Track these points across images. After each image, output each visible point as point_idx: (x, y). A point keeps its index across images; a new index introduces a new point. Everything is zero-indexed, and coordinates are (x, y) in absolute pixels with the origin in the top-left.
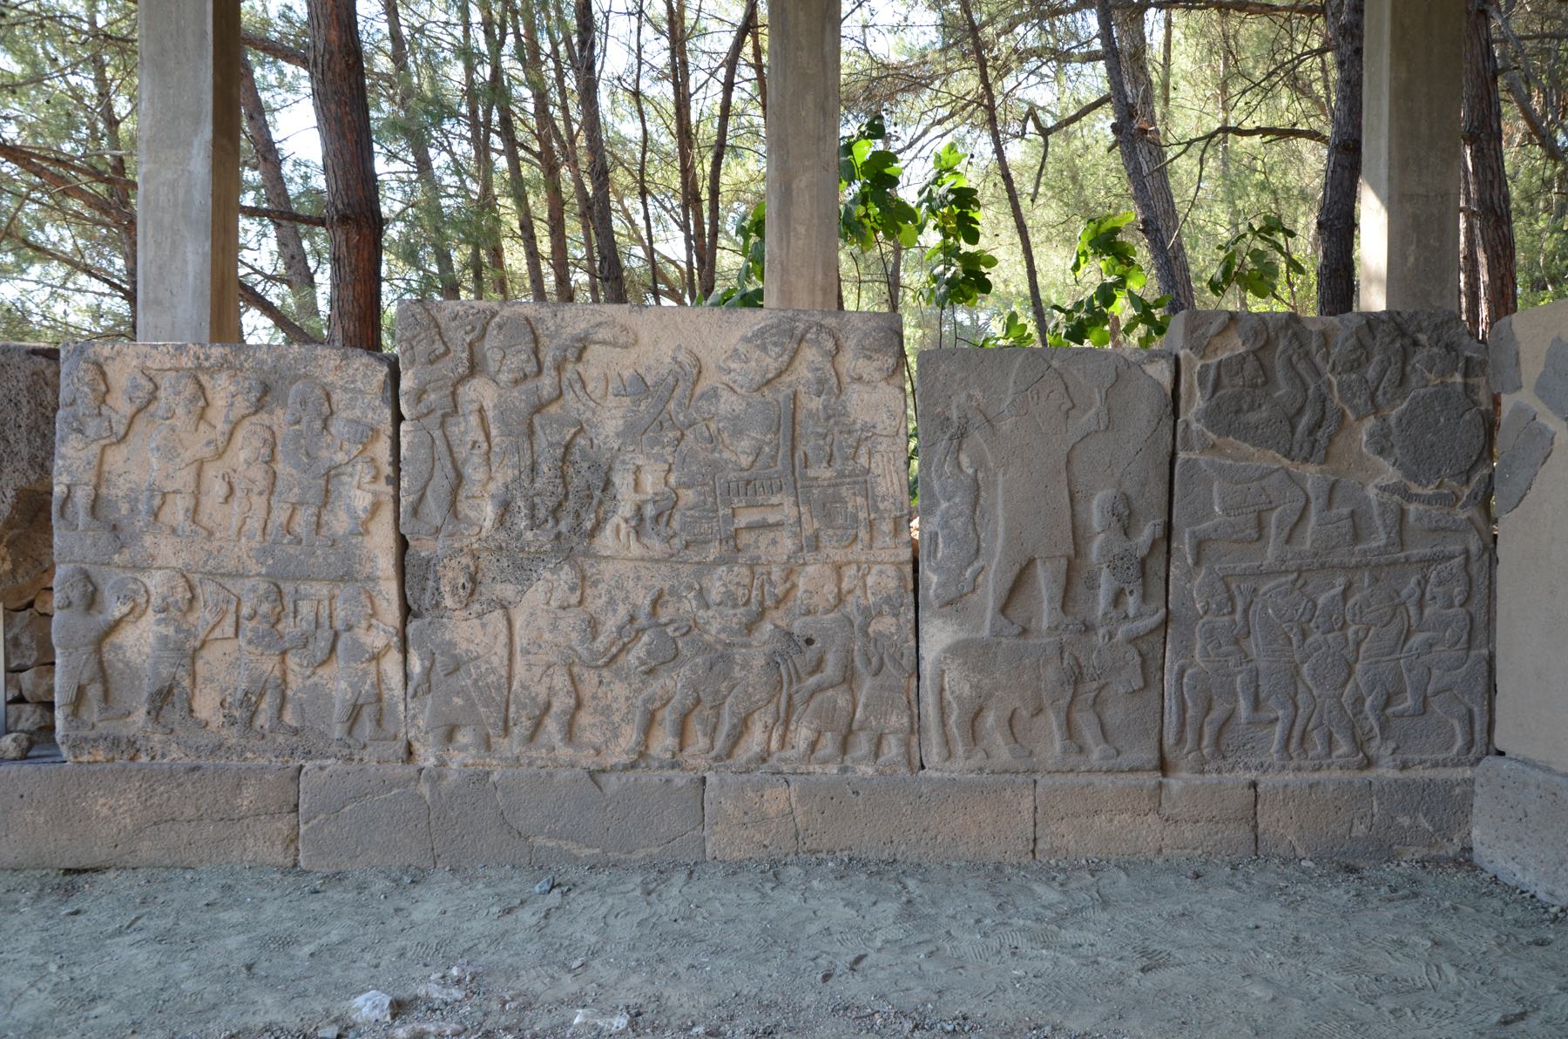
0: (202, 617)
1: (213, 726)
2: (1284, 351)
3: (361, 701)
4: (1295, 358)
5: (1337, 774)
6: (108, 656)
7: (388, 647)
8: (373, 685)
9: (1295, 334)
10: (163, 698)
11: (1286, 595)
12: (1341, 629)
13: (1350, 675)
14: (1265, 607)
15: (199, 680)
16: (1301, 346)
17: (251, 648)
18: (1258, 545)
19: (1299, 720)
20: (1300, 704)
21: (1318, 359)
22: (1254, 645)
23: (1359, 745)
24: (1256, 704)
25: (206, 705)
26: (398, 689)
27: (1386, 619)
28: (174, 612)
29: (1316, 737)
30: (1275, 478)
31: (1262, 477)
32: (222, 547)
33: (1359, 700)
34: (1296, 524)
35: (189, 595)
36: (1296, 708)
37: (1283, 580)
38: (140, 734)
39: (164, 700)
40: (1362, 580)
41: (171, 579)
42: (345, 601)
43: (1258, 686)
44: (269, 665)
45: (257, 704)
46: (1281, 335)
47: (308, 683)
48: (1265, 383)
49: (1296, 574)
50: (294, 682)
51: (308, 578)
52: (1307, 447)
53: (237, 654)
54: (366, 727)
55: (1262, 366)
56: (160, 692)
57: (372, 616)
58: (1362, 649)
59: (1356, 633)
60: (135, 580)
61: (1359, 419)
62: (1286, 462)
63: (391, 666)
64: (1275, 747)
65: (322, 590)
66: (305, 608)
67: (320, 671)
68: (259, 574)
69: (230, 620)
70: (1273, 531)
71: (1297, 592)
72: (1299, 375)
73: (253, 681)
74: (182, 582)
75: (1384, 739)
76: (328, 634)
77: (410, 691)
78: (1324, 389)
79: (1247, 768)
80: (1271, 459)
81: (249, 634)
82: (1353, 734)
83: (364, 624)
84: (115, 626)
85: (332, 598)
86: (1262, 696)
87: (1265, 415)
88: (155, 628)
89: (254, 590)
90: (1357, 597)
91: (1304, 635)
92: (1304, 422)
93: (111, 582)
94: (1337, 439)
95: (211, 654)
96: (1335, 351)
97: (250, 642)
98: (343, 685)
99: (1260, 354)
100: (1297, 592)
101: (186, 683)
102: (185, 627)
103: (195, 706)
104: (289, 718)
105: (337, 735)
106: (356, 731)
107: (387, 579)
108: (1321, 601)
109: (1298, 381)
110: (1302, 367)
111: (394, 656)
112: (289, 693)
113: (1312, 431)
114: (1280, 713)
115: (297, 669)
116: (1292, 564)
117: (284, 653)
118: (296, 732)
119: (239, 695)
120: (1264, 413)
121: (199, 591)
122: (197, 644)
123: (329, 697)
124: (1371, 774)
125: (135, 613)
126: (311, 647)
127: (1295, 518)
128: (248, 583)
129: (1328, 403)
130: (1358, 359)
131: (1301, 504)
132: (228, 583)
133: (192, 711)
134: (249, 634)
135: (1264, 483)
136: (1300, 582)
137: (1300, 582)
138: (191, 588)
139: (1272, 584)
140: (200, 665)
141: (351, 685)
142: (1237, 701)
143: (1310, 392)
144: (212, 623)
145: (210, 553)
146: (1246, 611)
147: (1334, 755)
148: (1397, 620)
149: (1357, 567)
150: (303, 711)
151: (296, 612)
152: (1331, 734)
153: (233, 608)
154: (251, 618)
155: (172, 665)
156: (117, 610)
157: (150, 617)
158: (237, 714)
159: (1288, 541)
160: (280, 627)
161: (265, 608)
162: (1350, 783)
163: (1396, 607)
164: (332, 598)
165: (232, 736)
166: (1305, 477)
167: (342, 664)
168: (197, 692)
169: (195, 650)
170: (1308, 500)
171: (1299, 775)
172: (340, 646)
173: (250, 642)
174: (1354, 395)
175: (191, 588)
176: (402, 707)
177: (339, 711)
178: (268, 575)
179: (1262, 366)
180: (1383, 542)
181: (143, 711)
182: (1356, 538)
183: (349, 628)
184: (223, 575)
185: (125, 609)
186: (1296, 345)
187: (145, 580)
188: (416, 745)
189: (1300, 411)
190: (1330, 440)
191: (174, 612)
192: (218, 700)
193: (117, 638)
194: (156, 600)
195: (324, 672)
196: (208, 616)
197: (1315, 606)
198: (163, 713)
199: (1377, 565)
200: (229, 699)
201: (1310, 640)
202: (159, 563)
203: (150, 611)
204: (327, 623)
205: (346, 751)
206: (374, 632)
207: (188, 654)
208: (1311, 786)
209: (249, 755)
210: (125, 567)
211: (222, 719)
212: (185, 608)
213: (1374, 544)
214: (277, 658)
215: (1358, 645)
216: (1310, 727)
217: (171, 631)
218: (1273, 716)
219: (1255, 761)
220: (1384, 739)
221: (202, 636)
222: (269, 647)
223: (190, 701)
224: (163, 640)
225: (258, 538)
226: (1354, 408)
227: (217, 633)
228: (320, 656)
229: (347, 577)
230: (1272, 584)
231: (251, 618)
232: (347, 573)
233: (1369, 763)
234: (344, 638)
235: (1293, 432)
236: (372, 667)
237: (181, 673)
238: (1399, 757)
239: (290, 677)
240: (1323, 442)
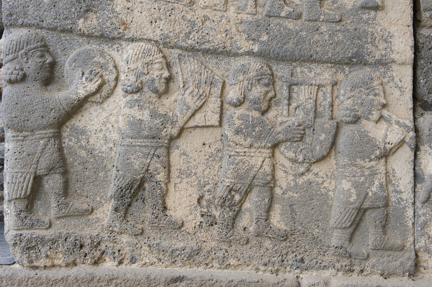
0: (176, 103)
1: (189, 226)
3: (367, 204)
6: (69, 142)
7: (402, 142)
8: (381, 186)
10: (132, 194)
15: (174, 173)
17: (239, 139)
25: (181, 203)
26: (407, 195)
28: (148, 94)
32: (206, 18)
35: (166, 74)
38: (105, 235)
39: (134, 196)
41: (147, 53)
42: (353, 88)
44: (258, 159)
45: (241, 202)
47: (301, 181)
50: (284, 180)
51: (310, 60)
53: (218, 145)
54: (370, 235)
56: (130, 186)
57: (384, 106)
60: (102, 54)
63: (401, 164)
65: (326, 75)
66: (303, 95)
67: (315, 169)
68: (250, 53)
69: (213, 104)
73: (239, 177)
74: (158, 58)
76: (329, 125)
77: (422, 193)
81: (238, 123)
83: (375, 115)
84: (78, 107)
85: (335, 84)
88: (127, 111)
89: (244, 70)
93: (72, 55)
95: (190, 144)
97: (238, 132)
98: (346, 185)
101: (161, 177)
102: (161, 111)
103: (169, 203)
104: (277, 220)
105: (334, 241)
106: (357, 238)
107: (403, 64)
111: (406, 153)
112: (278, 191)
115: (288, 164)
117: (275, 146)
118: (285, 237)
119: (221, 191)
121: (176, 69)
122: (175, 132)
123: (325, 199)
125: (99, 95)
126: (308, 140)
128: (236, 63)
132: (211, 62)
133: (165, 208)
134: (238, 123)
138: (169, 66)
140: (175, 155)
141: (356, 185)
144: (193, 107)
145: (193, 24)
150: (293, 211)
151: (290, 98)
153: (217, 91)
154: (239, 104)
155: (146, 155)
156: (78, 86)
157: (119, 99)
158: (217, 213)
160: (271, 114)
161: (257, 92)
164: (335, 84)
165: (210, 239)
167: (344, 160)
168: (171, 187)
169: (172, 139)
172: (342, 140)
173: (238, 132)
175: (169, 66)
176: (410, 213)
177: (337, 215)
178: (260, 55)
181: (109, 207)
183: (356, 120)
184: (206, 52)
185: (92, 87)
187: (114, 53)
188: (423, 256)
191: (148, 94)
192: (196, 197)
193: (80, 121)
194: (127, 79)
195: (321, 169)
196: (188, 99)
198: (132, 209)
200: (207, 197)
202: (129, 35)
203: (119, 90)
204: (327, 113)
205: (346, 262)
206: (383, 125)
207: (163, 140)
209: (233, 262)
210: (90, 36)
211: (199, 219)
212: (162, 89)
214: (267, 152)
217: (145, 115)
221: (180, 123)
222: (258, 138)
223: (164, 196)
224: (136, 125)
225: (249, 9)
227: (199, 119)
228: (319, 150)
229: (356, 60)
231: (239, 104)
232: (356, 55)
234: (347, 131)
236: (381, 166)
237: (156, 165)
239: (280, 174)
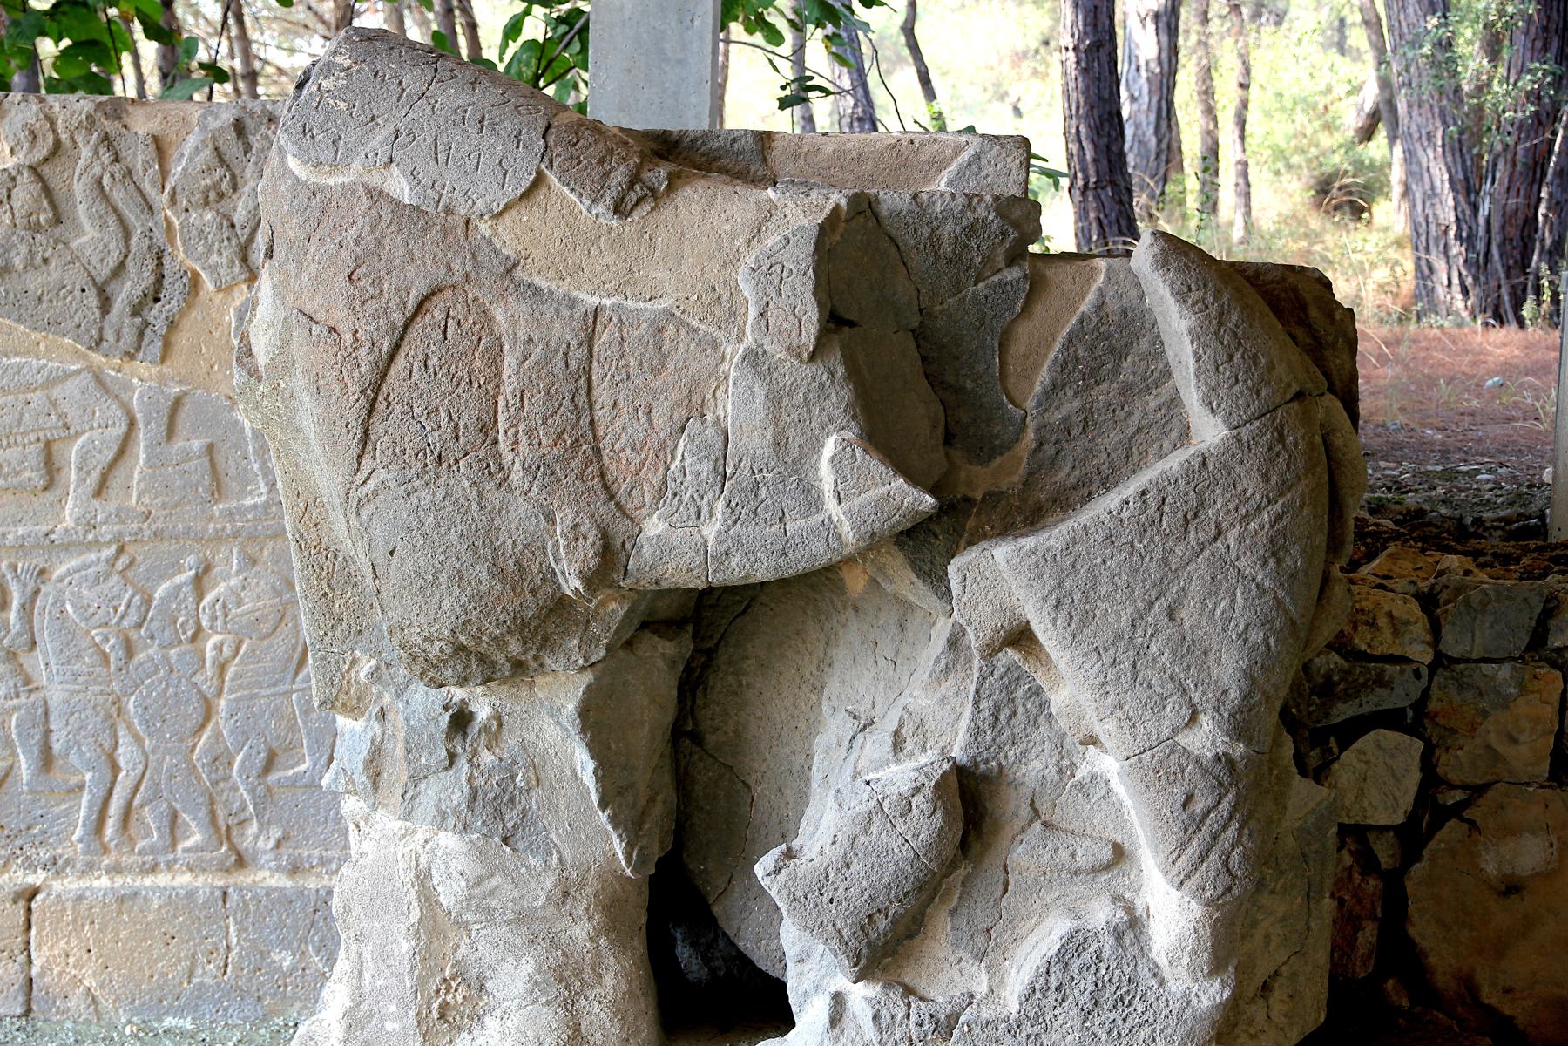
2: (87, 168)
4: (106, 181)
5: (184, 879)
9: (106, 139)
11: (97, 581)
12: (194, 639)
13: (207, 717)
14: (58, 602)
16: (117, 160)
18: (50, 497)
19: (118, 789)
20: (122, 762)
21: (147, 186)
22: (44, 665)
23: (223, 832)
24: (46, 759)
27: (265, 628)
29: (150, 818)
30: (72, 388)
31: (50, 383)
33: (220, 760)
34: (112, 465)
36: (115, 768)
37: (93, 556)
40: (228, 561)
43: (48, 732)
46: (79, 139)
48: (58, 220)
49: (113, 548)
52: (129, 334)
55: (47, 191)
58: (231, 670)
59: (219, 648)
61: (225, 289)
62: (97, 358)
64: (79, 832)
70: (73, 477)
71: (116, 578)
72: (115, 210)
75: (264, 827)
78: (160, 238)
79: (31, 866)
80: (62, 355)
82: (213, 813)
86: (57, 747)
87: (55, 275)
90: (221, 588)
91: (129, 649)
92: (126, 292)
94: (186, 324)
96: (177, 170)
99: (46, 171)
100: (116, 578)
108: (160, 592)
109: (111, 219)
110: (118, 195)
113: (136, 311)
114: (88, 776)
116: (106, 532)
120: (54, 272)
124: (245, 878)
127: (110, 455)
129: (166, 260)
130: (216, 185)
131: (122, 429)
135: (56, 392)
136: (123, 561)
137: (123, 561)
139: (74, 563)
142: (14, 754)
143: (134, 241)
146: (27, 609)
147: (180, 847)
148: (284, 630)
149: (218, 538)
152: (174, 816)
159: (100, 490)
162: (191, 894)
163: (285, 605)
166: (129, 387)
170: (132, 424)
171: (119, 881)
174: (210, 250)
179: (47, 191)
180: (263, 498)
182: (217, 488)
186: (106, 158)
189: (119, 270)
190: (172, 324)
197: (148, 602)
199: (252, 537)
201: (142, 656)
208: (121, 900)
213: (248, 502)
215: (222, 668)
216: (136, 802)
218: (74, 780)
219: (44, 854)
220: (264, 827)
226: (213, 269)
230: (74, 563)
233: (241, 862)
235: (105, 305)
238: (286, 853)
240: (160, 326)
